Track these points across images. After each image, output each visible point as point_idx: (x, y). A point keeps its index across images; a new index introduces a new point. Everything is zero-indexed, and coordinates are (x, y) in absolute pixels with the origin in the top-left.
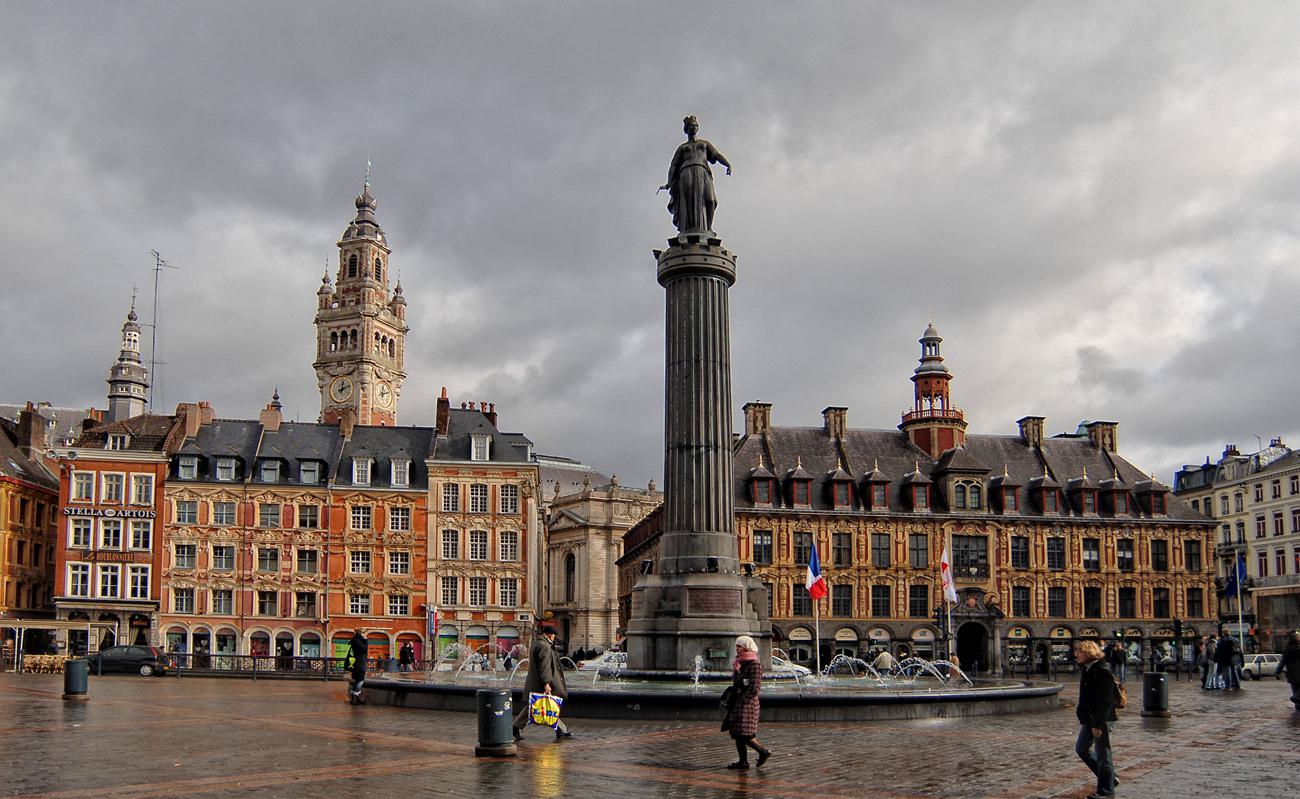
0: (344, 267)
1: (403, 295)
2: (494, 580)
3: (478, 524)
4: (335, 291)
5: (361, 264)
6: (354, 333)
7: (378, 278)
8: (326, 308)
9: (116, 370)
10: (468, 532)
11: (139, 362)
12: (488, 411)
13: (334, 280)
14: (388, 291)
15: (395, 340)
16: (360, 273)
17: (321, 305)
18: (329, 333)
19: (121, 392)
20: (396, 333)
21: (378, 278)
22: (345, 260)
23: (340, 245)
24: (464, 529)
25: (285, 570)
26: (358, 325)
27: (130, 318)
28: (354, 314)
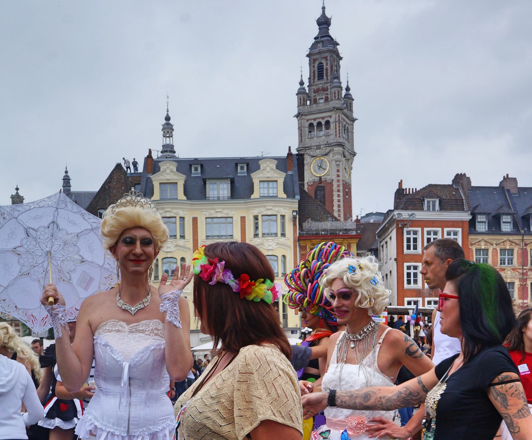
1: (351, 92)
4: (307, 91)
6: (328, 123)
8: (304, 104)
17: (300, 103)
18: (307, 124)
22: (314, 67)
23: (308, 56)
26: (331, 117)
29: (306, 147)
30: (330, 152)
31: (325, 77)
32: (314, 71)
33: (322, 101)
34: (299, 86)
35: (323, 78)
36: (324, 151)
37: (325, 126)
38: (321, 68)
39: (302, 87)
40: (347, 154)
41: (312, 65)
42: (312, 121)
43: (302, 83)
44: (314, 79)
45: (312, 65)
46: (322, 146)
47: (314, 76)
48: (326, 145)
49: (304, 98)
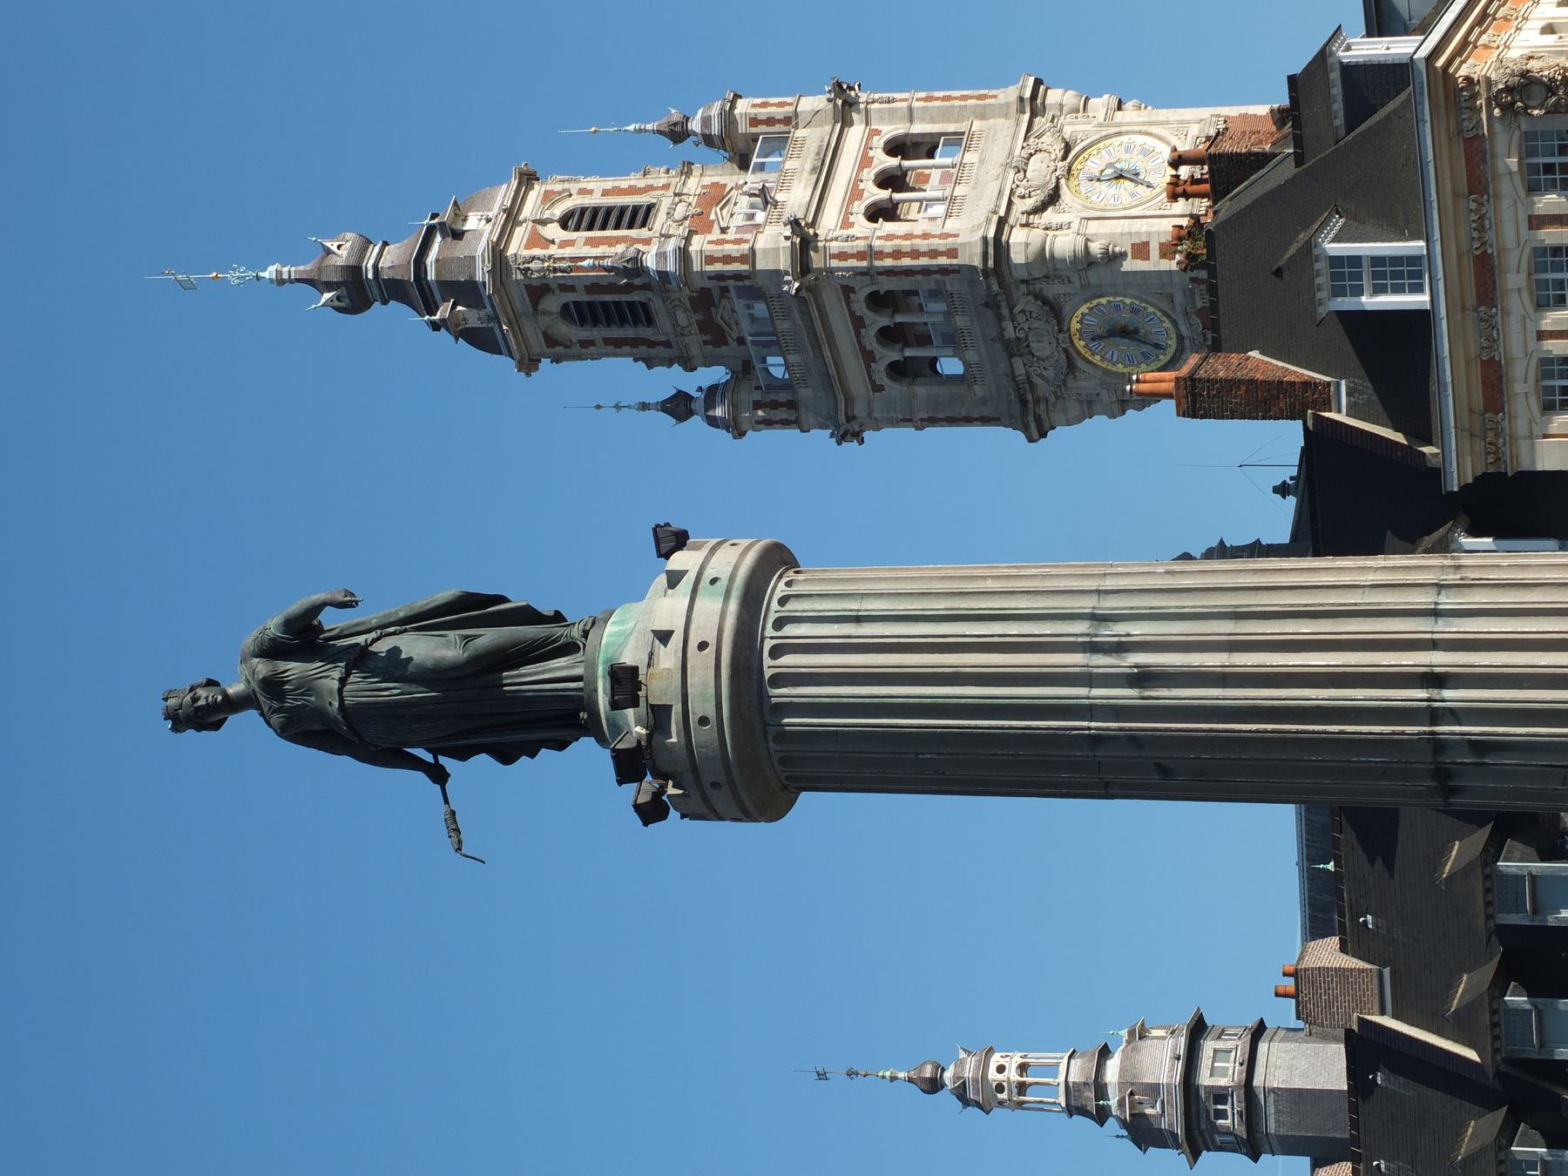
0: (616, 346)
4: (717, 374)
5: (594, 287)
6: (878, 301)
7: (639, 216)
9: (1142, 1133)
11: (1105, 1053)
13: (671, 379)
15: (890, 130)
16: (629, 288)
17: (785, 423)
18: (895, 389)
19: (1231, 1120)
20: (855, 134)
21: (639, 216)
22: (585, 344)
23: (528, 365)
26: (847, 290)
28: (806, 314)
29: (1024, 402)
31: (636, 297)
32: (607, 342)
33: (760, 309)
34: (696, 422)
35: (644, 306)
36: (1036, 324)
37: (897, 311)
38: (583, 313)
39: (698, 406)
40: (1040, 170)
42: (880, 368)
43: (679, 407)
44: (652, 344)
45: (577, 349)
46: (1010, 333)
47: (634, 343)
49: (757, 405)
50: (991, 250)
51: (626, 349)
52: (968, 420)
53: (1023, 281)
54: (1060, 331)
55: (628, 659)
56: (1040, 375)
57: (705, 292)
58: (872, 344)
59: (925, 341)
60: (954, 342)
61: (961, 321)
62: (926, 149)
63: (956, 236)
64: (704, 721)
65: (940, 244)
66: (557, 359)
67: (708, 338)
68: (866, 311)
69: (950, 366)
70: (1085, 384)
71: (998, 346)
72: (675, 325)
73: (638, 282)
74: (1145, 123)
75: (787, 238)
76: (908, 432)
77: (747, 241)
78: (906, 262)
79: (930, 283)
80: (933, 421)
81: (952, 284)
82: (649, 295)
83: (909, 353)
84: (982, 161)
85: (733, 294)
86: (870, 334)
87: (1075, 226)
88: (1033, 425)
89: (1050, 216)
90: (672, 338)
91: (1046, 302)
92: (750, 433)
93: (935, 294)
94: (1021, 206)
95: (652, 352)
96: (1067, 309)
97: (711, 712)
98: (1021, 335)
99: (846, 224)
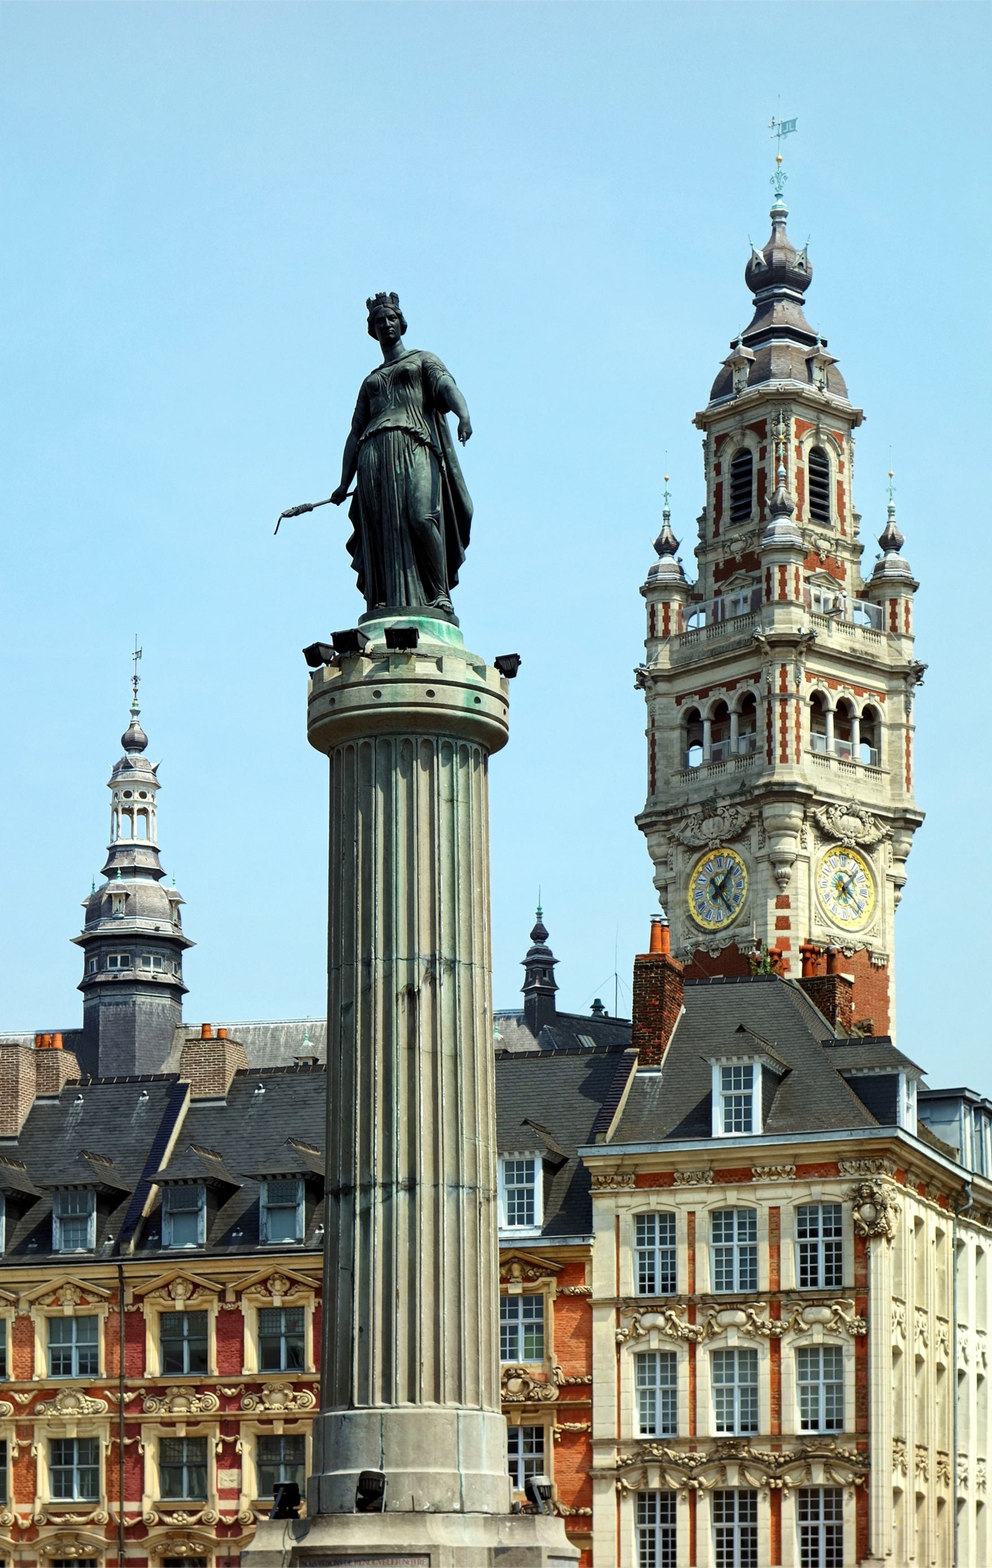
2: (776, 1497)
3: (734, 1330)
4: (692, 575)
6: (748, 702)
10: (703, 1356)
12: (822, 972)
13: (688, 537)
14: (858, 550)
16: (762, 503)
17: (652, 628)
18: (677, 715)
22: (718, 468)
24: (693, 1345)
25: (227, 1494)
26: (756, 677)
27: (132, 744)
29: (666, 813)
30: (749, 825)
31: (755, 509)
32: (719, 486)
33: (744, 609)
35: (748, 515)
36: (727, 823)
37: (740, 716)
41: (713, 460)
42: (695, 702)
44: (717, 521)
45: (713, 460)
46: (721, 803)
47: (718, 508)
48: (732, 796)
50: (786, 788)
51: (713, 501)
52: (653, 770)
53: (761, 813)
54: (722, 841)
55: (423, 639)
56: (687, 826)
57: (757, 565)
58: (714, 696)
59: (716, 737)
60: (716, 759)
61: (731, 766)
62: (868, 737)
63: (798, 762)
64: (378, 694)
65: (790, 751)
66: (706, 444)
67: (721, 564)
68: (740, 692)
69: (696, 757)
70: (680, 862)
71: (711, 794)
72: (733, 541)
73: (767, 511)
74: (884, 905)
75: (799, 630)
76: (644, 724)
77: (797, 598)
78: (778, 724)
79: (761, 742)
80: (653, 743)
81: (760, 759)
82: (757, 520)
83: (707, 726)
84: (857, 781)
85: (756, 587)
86: (722, 694)
87: (804, 853)
88: (648, 820)
89: (810, 835)
90: (721, 538)
91: (745, 830)
92: (645, 600)
93: (753, 744)
94: (820, 812)
95: (711, 522)
96: (738, 847)
97: (384, 699)
98: (719, 811)
99: (810, 675)
